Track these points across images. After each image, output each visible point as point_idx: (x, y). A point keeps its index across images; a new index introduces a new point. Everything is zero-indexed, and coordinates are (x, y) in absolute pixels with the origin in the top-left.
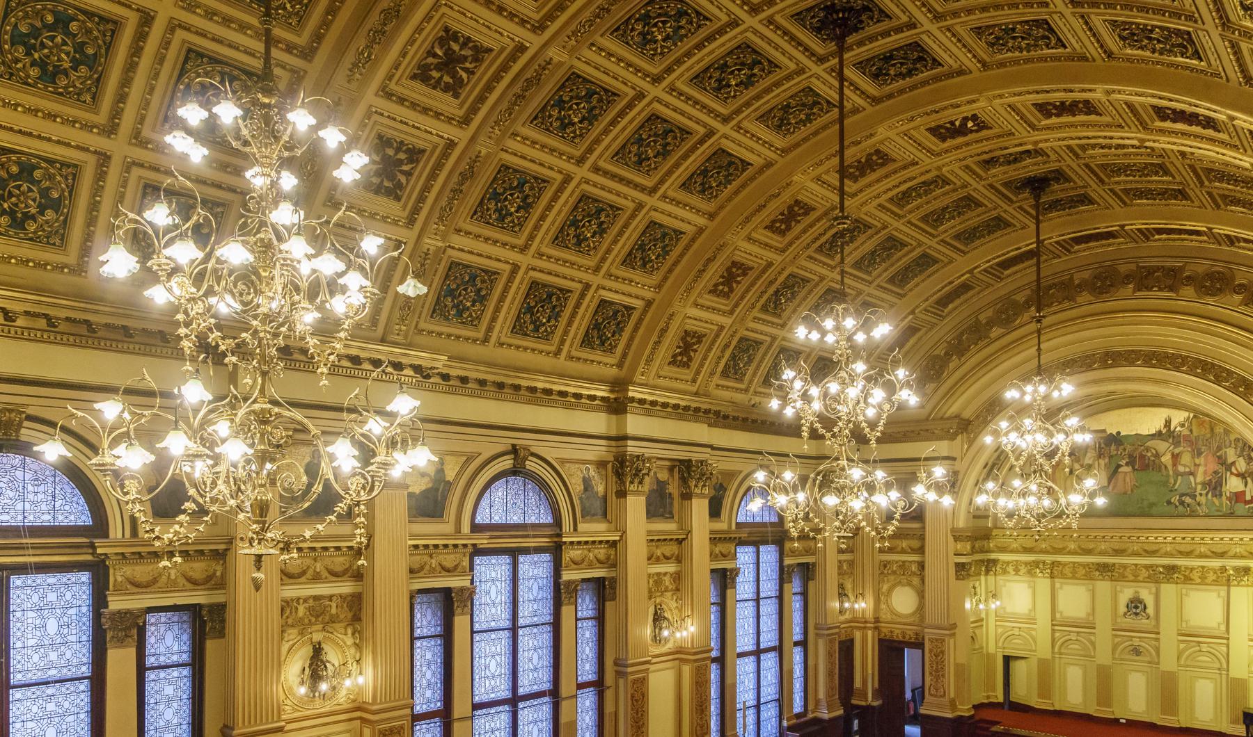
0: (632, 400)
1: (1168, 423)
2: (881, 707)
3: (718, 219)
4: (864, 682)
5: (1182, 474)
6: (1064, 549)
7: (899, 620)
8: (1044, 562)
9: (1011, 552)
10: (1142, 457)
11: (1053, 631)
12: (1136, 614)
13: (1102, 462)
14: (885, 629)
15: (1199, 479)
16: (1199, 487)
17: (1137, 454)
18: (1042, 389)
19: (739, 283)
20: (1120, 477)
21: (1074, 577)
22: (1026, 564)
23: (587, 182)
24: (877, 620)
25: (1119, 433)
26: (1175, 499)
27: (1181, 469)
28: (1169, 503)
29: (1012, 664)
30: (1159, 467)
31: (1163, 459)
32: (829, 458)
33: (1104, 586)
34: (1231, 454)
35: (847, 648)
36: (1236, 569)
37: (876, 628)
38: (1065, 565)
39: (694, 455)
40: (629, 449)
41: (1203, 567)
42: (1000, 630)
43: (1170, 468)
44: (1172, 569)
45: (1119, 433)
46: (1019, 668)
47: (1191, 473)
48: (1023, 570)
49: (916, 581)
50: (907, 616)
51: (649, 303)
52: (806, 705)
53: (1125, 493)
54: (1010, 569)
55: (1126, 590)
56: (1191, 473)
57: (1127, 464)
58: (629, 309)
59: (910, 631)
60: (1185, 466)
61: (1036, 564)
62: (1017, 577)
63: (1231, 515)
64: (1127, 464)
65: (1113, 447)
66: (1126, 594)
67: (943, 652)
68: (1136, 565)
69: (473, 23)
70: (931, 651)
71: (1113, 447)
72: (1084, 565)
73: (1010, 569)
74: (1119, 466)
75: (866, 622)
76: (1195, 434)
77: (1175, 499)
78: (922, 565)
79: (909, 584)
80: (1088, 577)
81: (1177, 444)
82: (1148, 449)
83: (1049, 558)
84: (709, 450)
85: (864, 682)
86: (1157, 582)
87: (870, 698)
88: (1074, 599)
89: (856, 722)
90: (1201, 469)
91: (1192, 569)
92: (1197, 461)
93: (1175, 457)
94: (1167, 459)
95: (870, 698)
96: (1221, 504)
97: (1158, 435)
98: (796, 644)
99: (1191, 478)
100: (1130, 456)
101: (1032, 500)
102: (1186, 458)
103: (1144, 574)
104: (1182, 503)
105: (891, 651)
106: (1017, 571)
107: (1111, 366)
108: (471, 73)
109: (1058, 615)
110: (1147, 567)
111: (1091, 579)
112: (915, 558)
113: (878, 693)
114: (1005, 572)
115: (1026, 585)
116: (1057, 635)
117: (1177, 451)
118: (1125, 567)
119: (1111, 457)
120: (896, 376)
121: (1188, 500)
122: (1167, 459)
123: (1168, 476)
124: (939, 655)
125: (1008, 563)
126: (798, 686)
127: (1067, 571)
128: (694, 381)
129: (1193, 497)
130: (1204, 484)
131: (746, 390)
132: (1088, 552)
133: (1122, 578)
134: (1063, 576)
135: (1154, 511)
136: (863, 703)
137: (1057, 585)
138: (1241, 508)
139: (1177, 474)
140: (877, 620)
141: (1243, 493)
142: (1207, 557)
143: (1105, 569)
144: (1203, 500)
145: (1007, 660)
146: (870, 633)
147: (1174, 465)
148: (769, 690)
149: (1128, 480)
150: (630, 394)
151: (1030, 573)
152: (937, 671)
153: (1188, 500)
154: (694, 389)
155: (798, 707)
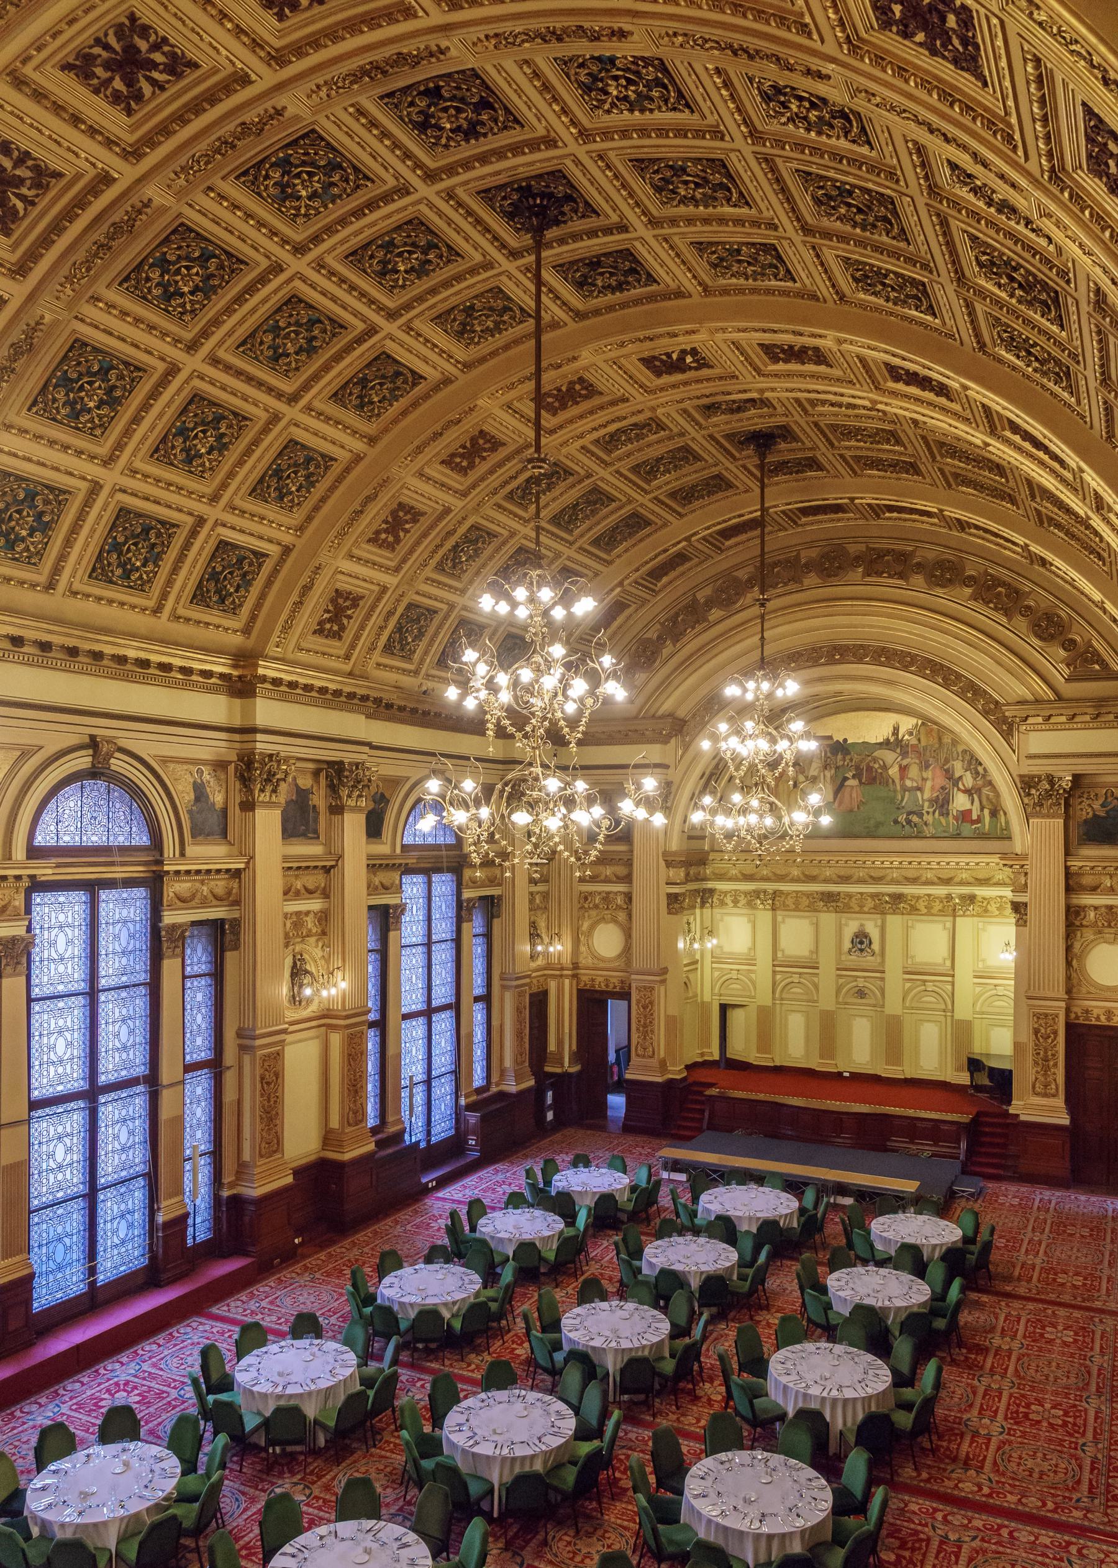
0: (263, 679)
1: (896, 730)
2: (580, 1073)
3: (381, 445)
4: (560, 1043)
5: (910, 790)
6: (787, 875)
7: (602, 965)
8: (765, 892)
9: (730, 879)
10: (870, 769)
11: (774, 972)
12: (862, 950)
13: (828, 774)
14: (585, 977)
15: (926, 796)
16: (926, 804)
17: (864, 766)
18: (765, 686)
19: (407, 531)
20: (848, 790)
21: (797, 909)
22: (746, 894)
23: (201, 377)
24: (576, 966)
25: (845, 740)
26: (902, 818)
27: (908, 783)
28: (896, 822)
29: (729, 1013)
30: (886, 781)
31: (890, 772)
32: (521, 763)
33: (828, 919)
34: (958, 768)
35: (539, 1003)
36: (962, 897)
37: (575, 976)
38: (788, 894)
39: (347, 755)
40: (258, 745)
41: (929, 895)
42: (716, 974)
43: (897, 781)
44: (898, 898)
45: (845, 740)
46: (737, 1018)
47: (919, 789)
48: (743, 901)
50: (610, 960)
51: (287, 550)
52: (488, 1077)
53: (851, 811)
54: (728, 900)
55: (851, 923)
56: (919, 789)
57: (854, 777)
58: (260, 556)
59: (615, 979)
60: (912, 780)
61: (757, 894)
62: (736, 910)
63: (957, 836)
64: (854, 777)
65: (840, 756)
66: (851, 927)
67: (651, 1003)
68: (862, 894)
69: (34, 133)
70: (638, 1002)
71: (840, 756)
72: (808, 895)
73: (728, 900)
74: (845, 779)
75: (562, 969)
76: (923, 743)
77: (902, 818)
81: (904, 754)
82: (875, 760)
83: (770, 887)
84: (366, 749)
85: (560, 1043)
86: (883, 913)
87: (566, 1064)
88: (798, 935)
89: (550, 1094)
90: (929, 784)
91: (918, 898)
92: (925, 775)
93: (903, 769)
94: (894, 771)
95: (566, 1064)
96: (948, 824)
97: (886, 744)
98: (477, 999)
99: (919, 794)
100: (857, 768)
101: (753, 819)
102: (914, 771)
103: (870, 903)
104: (909, 822)
105: (592, 1005)
106: (736, 902)
107: (839, 662)
108: (30, 203)
109: (779, 954)
110: (874, 896)
111: (816, 911)
113: (576, 1057)
114: (722, 903)
115: (745, 919)
116: (778, 977)
117: (905, 763)
118: (850, 896)
119: (837, 768)
120: (600, 664)
121: (915, 819)
122: (894, 771)
123: (895, 791)
124: (648, 1006)
125: (726, 893)
126: (479, 1052)
127: (790, 901)
128: (347, 657)
129: (921, 815)
130: (930, 801)
131: (416, 672)
132: (812, 879)
133: (846, 909)
134: (786, 907)
135: (882, 830)
136: (558, 1070)
137: (779, 918)
138: (967, 829)
139: (905, 789)
140: (576, 966)
141: (970, 811)
142: (933, 883)
143: (829, 899)
144: (929, 818)
145: (724, 1008)
146: (567, 982)
147: (902, 778)
148: (443, 1061)
150: (261, 671)
151: (750, 905)
152: (645, 1026)
153: (915, 819)
154: (347, 668)
155: (478, 1081)
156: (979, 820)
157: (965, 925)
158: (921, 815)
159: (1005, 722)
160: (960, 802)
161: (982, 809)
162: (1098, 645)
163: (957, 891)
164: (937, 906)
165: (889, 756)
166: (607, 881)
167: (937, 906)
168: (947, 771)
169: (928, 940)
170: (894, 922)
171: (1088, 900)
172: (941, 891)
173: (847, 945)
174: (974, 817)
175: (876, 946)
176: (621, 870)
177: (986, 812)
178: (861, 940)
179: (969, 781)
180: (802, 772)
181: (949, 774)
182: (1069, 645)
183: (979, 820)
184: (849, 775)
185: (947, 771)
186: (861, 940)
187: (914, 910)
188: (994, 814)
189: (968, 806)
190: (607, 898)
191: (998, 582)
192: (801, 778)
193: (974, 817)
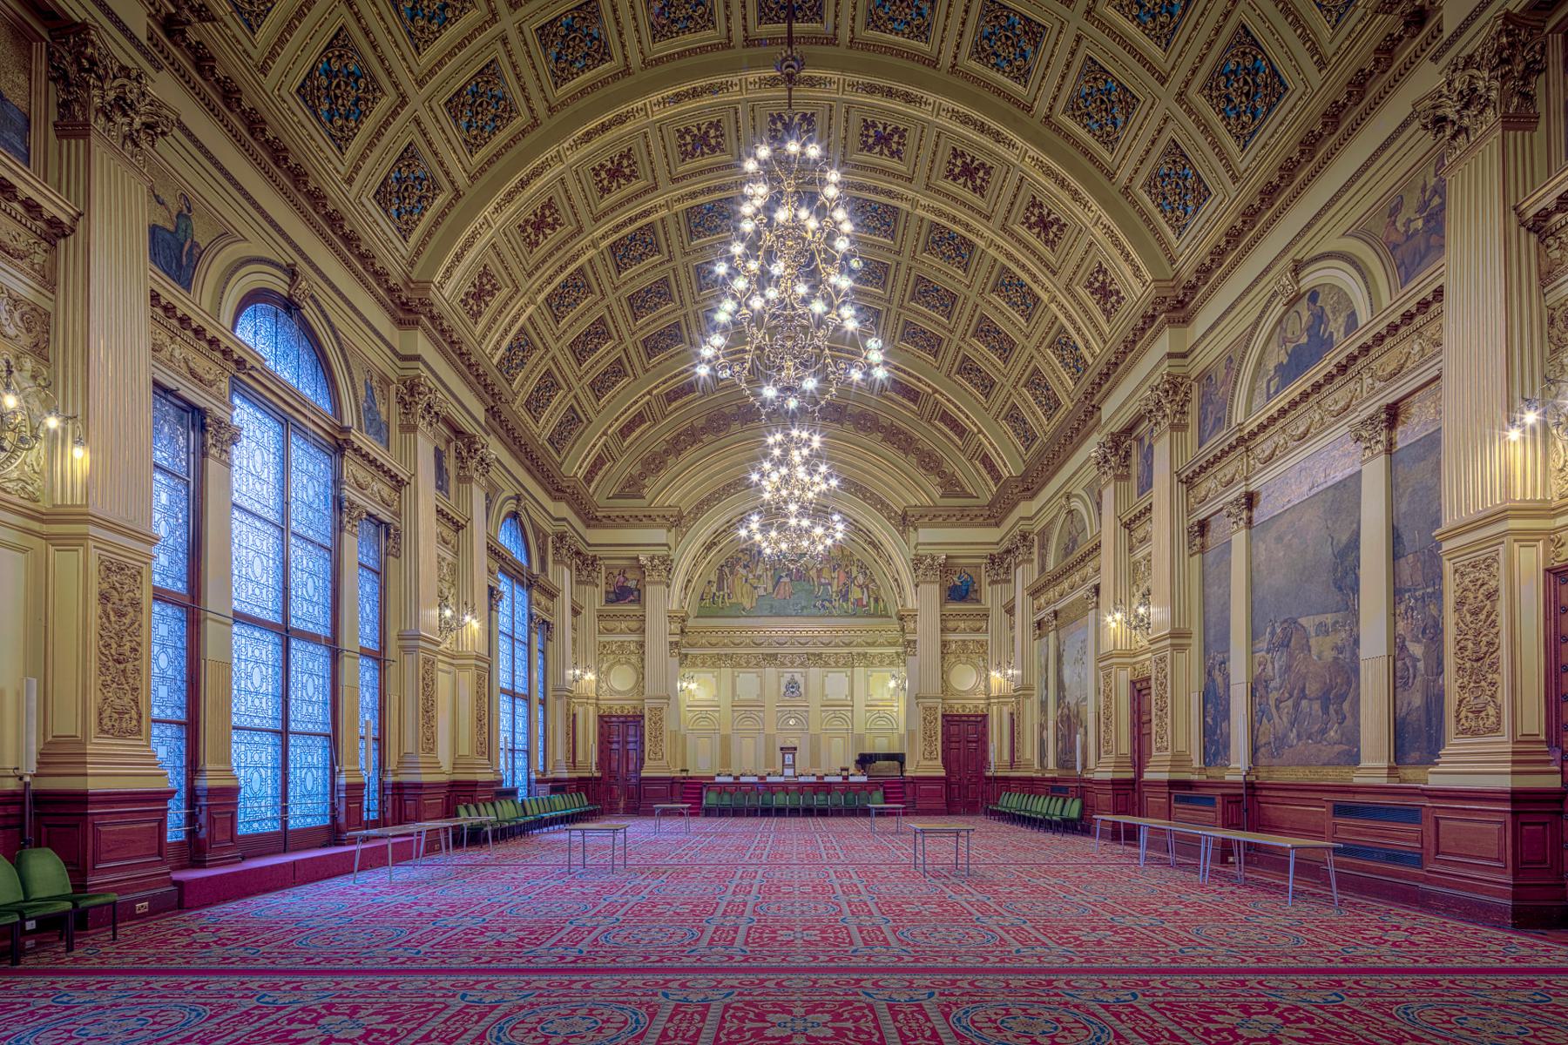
30: (809, 580)
33: (771, 672)
49: (634, 659)
54: (698, 661)
66: (788, 677)
73: (698, 661)
78: (641, 645)
79: (628, 662)
80: (757, 665)
88: (748, 683)
94: (813, 573)
102: (825, 573)
106: (704, 663)
112: (634, 638)
114: (694, 665)
127: (743, 662)
134: (740, 665)
138: (860, 611)
139: (820, 584)
157: (860, 672)
159: (905, 521)
160: (856, 593)
162: (959, 475)
163: (855, 650)
164: (842, 661)
166: (622, 632)
167: (842, 661)
169: (835, 683)
170: (814, 672)
172: (846, 650)
173: (783, 689)
175: (802, 689)
176: (634, 625)
178: (792, 686)
179: (861, 579)
182: (942, 474)
183: (868, 604)
186: (792, 686)
187: (827, 664)
188: (876, 600)
190: (622, 645)
191: (900, 431)
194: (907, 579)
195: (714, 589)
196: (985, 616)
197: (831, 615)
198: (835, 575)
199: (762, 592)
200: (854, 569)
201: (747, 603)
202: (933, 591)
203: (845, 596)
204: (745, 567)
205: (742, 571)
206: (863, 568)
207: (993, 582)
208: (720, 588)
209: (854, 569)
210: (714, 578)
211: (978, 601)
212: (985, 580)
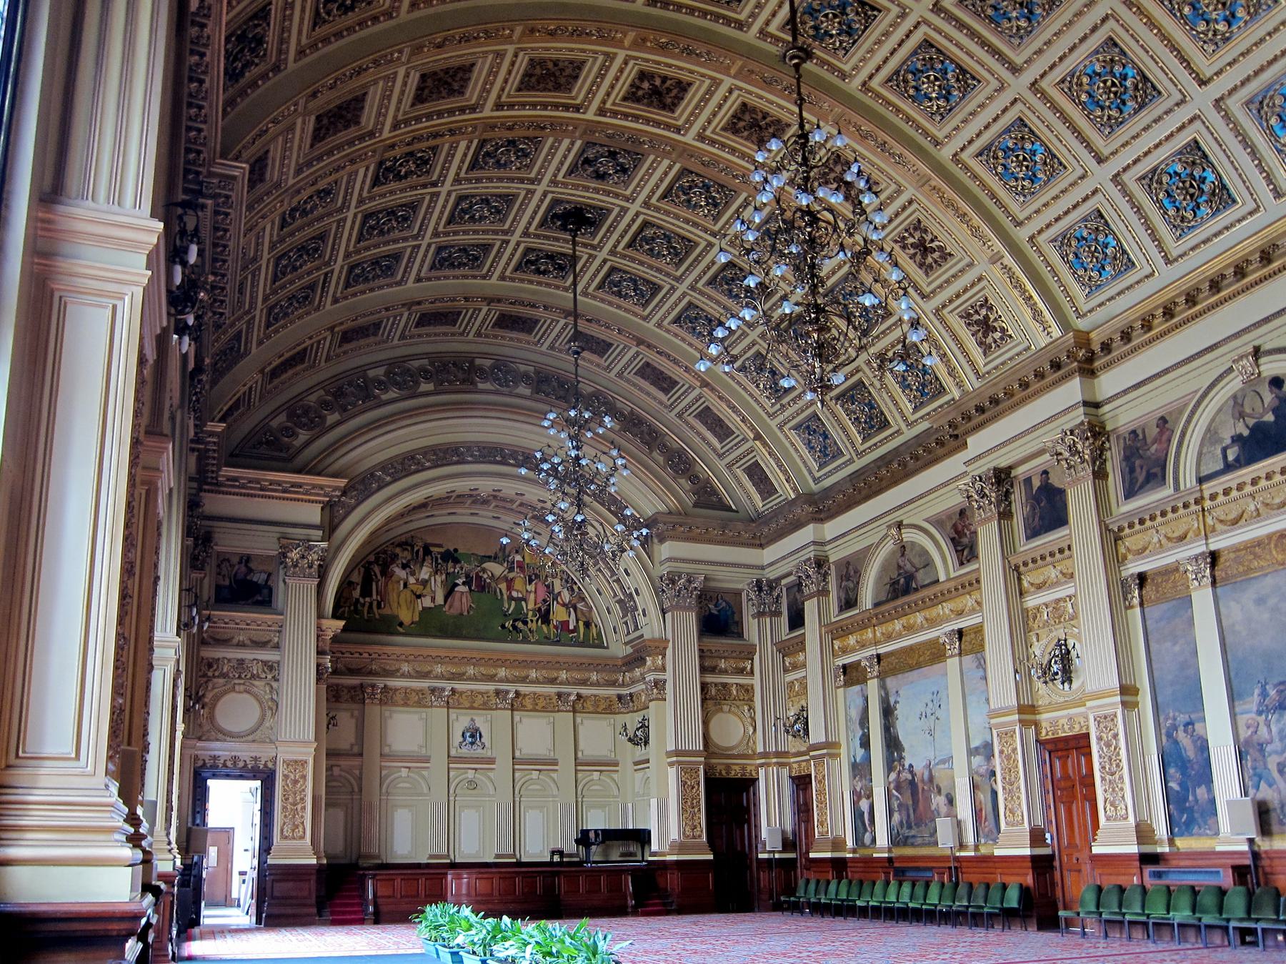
10: (479, 578)
13: (439, 578)
16: (530, 613)
20: (457, 596)
25: (456, 550)
27: (515, 594)
28: (503, 626)
43: (504, 591)
45: (456, 550)
57: (464, 583)
64: (464, 583)
65: (450, 564)
71: (450, 564)
74: (457, 585)
76: (527, 560)
81: (511, 569)
82: (484, 570)
92: (529, 588)
96: (549, 630)
100: (467, 576)
102: (518, 584)
117: (511, 575)
119: (448, 574)
121: (520, 625)
130: (533, 610)
139: (511, 598)
144: (533, 626)
147: (509, 588)
149: (464, 600)
153: (520, 625)
156: (576, 630)
158: (525, 623)
160: (559, 614)
161: (577, 621)
165: (496, 569)
168: (548, 586)
171: (710, 678)
174: (571, 627)
177: (581, 624)
179: (566, 596)
180: (413, 574)
181: (550, 588)
183: (576, 630)
184: (460, 581)
185: (548, 586)
188: (587, 625)
189: (566, 618)
192: (412, 580)
193: (571, 627)
194: (646, 600)
195: (356, 593)
196: (749, 653)
197: (525, 640)
198: (531, 588)
199: (427, 602)
200: (557, 583)
201: (406, 616)
202: (689, 621)
203: (545, 617)
204: (404, 567)
205: (400, 573)
206: (569, 583)
207: (760, 614)
208: (366, 592)
209: (557, 583)
210: (356, 578)
211: (740, 635)
212: (748, 611)
